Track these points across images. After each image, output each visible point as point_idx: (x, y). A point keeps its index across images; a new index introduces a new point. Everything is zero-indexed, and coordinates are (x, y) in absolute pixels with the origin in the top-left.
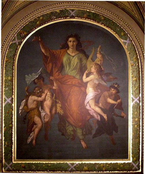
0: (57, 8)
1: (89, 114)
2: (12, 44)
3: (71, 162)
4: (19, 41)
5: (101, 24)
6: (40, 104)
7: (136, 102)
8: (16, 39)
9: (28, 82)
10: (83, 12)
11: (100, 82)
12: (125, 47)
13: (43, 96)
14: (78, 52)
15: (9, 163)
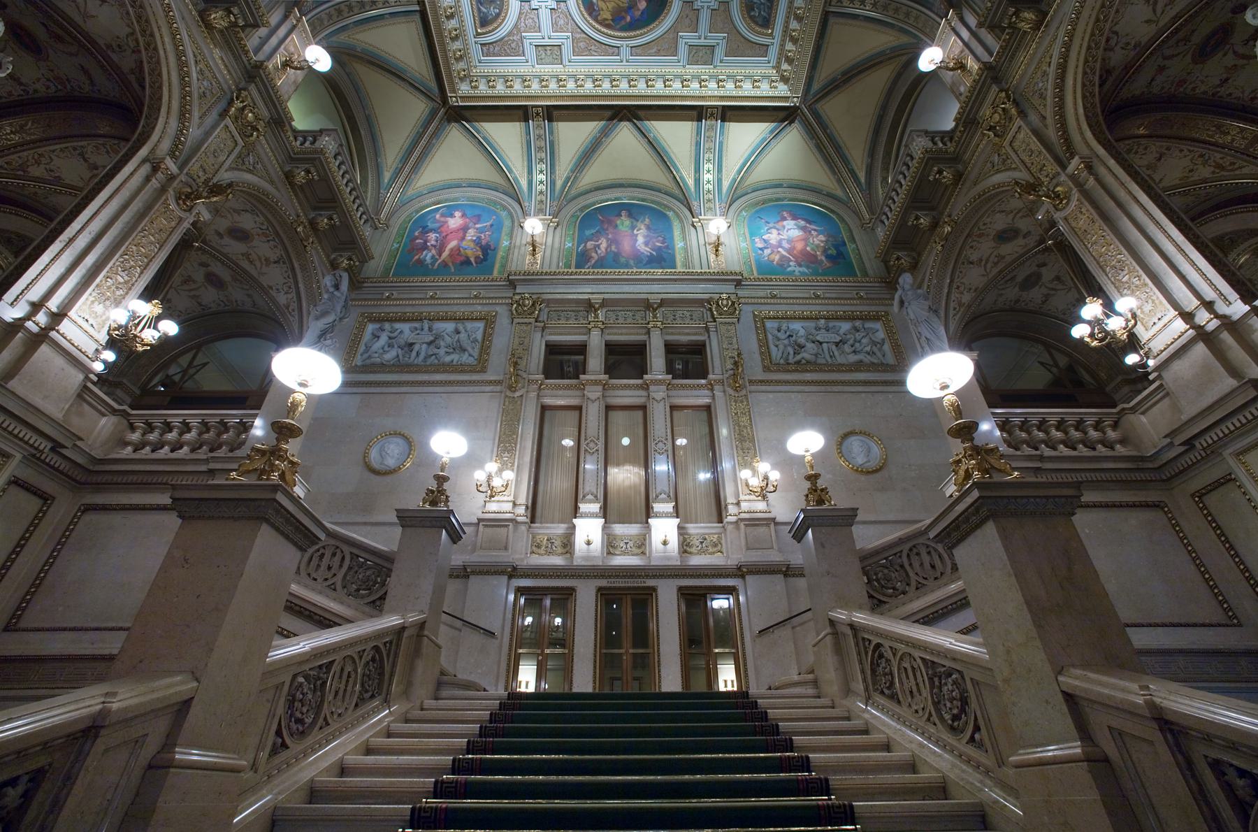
6: (598, 246)
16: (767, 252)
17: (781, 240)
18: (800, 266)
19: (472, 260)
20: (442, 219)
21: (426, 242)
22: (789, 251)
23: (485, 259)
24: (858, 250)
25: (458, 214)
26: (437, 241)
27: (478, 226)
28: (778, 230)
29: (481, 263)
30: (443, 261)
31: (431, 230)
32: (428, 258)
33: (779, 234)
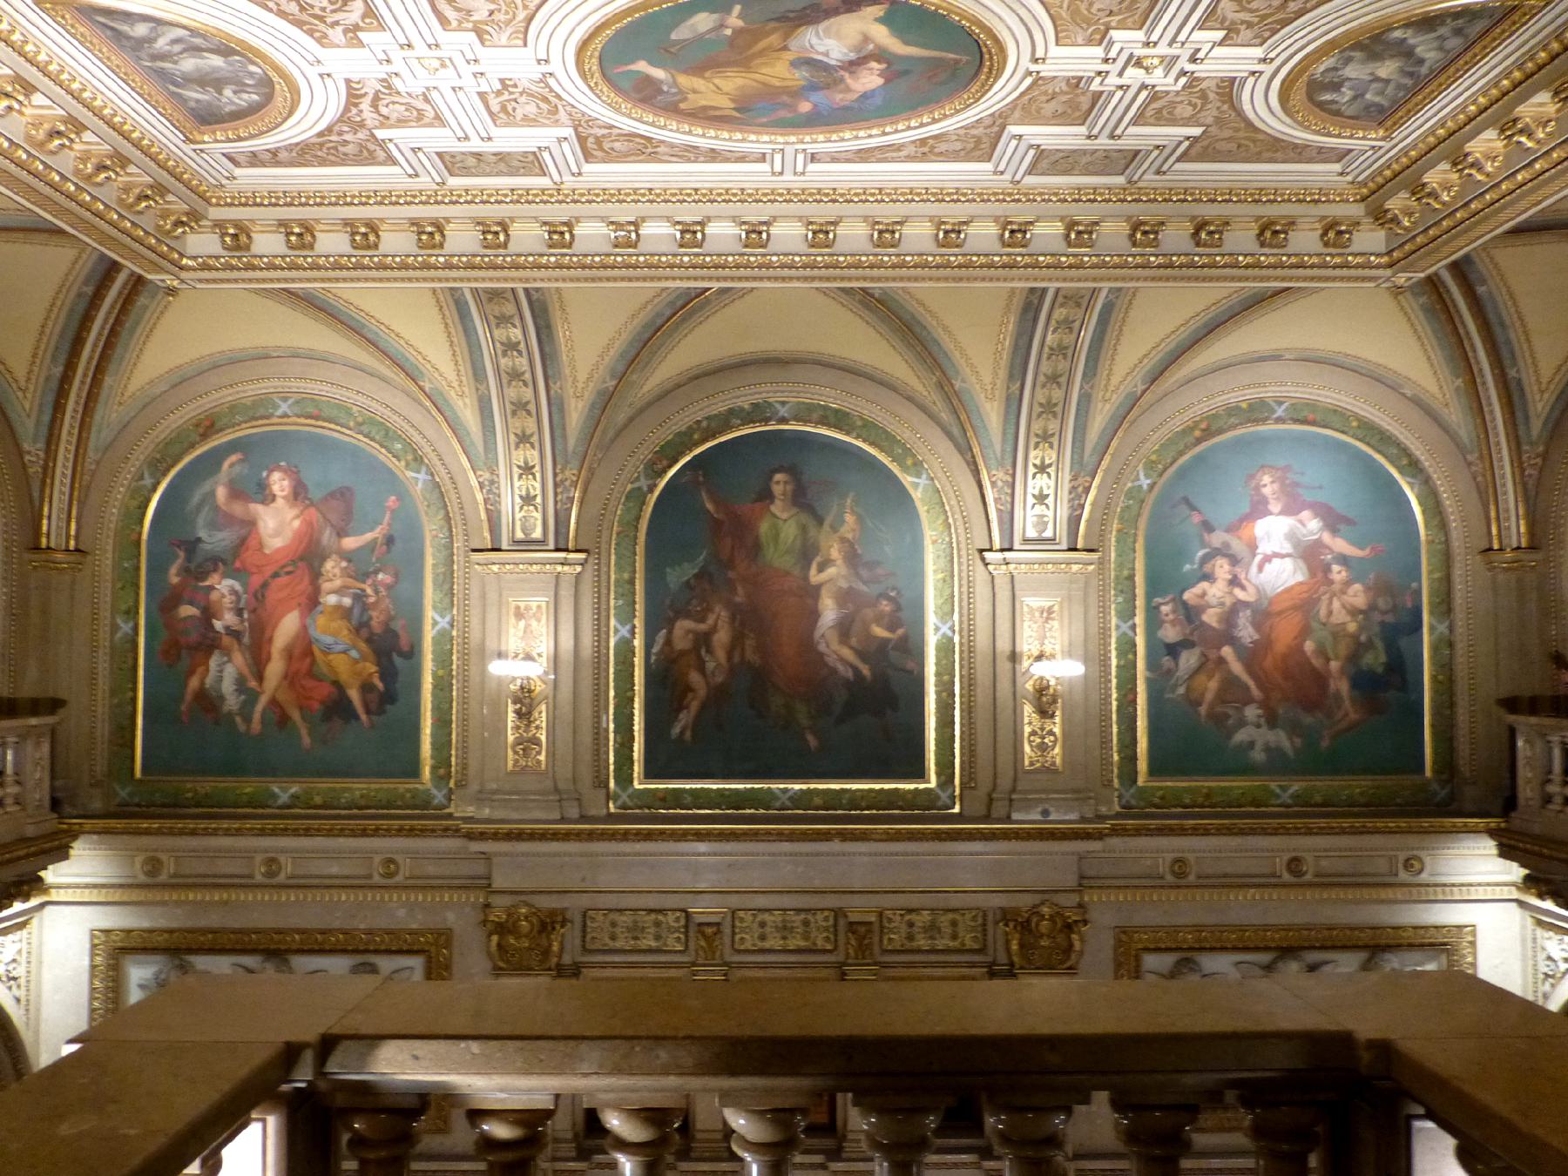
0: (743, 399)
1: (826, 665)
2: (632, 490)
3: (782, 786)
4: (650, 482)
5: (856, 438)
6: (703, 640)
7: (944, 635)
8: (642, 479)
9: (672, 586)
10: (811, 408)
11: (854, 585)
12: (917, 495)
13: (711, 621)
14: (795, 510)
15: (624, 789)
16: (1189, 660)
17: (1238, 605)
18: (1272, 720)
19: (354, 695)
20: (238, 509)
21: (208, 613)
22: (1251, 657)
23: (389, 697)
24: (1451, 645)
25: (279, 483)
26: (239, 612)
27: (350, 543)
28: (1234, 560)
29: (381, 711)
30: (273, 702)
31: (216, 562)
32: (228, 687)
33: (1234, 582)
